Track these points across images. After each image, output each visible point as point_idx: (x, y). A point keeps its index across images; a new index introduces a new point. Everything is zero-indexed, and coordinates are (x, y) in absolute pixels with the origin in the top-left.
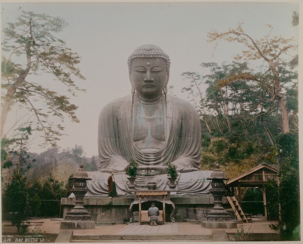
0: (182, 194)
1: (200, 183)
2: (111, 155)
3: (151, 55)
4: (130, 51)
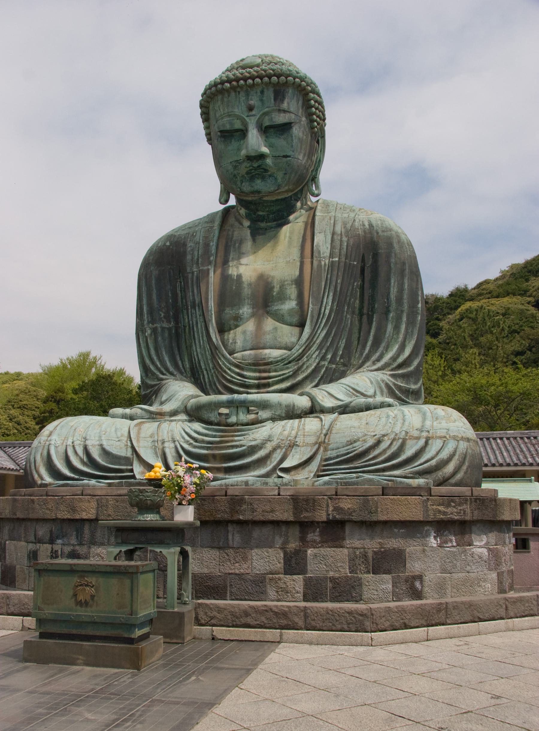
0: (327, 478)
1: (394, 443)
2: (161, 376)
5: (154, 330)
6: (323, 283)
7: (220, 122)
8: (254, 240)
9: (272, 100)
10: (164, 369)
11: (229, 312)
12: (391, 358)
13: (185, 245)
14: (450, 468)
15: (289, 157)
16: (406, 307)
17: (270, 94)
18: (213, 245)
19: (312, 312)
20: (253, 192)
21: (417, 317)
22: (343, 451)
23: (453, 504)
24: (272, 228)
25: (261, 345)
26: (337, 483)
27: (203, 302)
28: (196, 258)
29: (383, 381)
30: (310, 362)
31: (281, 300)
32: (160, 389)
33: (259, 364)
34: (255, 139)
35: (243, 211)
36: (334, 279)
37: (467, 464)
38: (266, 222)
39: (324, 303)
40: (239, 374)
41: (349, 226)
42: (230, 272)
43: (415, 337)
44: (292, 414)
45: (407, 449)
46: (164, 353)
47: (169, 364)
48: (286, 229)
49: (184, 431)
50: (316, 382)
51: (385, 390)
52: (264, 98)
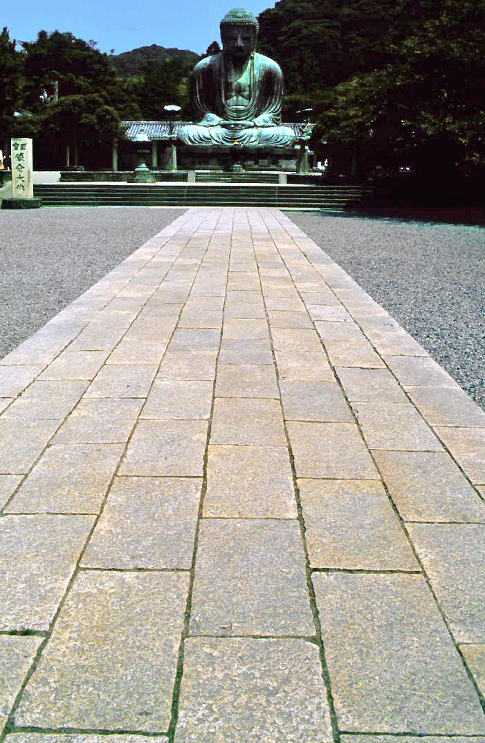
14: (288, 143)
17: (245, 29)
33: (238, 111)
44: (250, 127)
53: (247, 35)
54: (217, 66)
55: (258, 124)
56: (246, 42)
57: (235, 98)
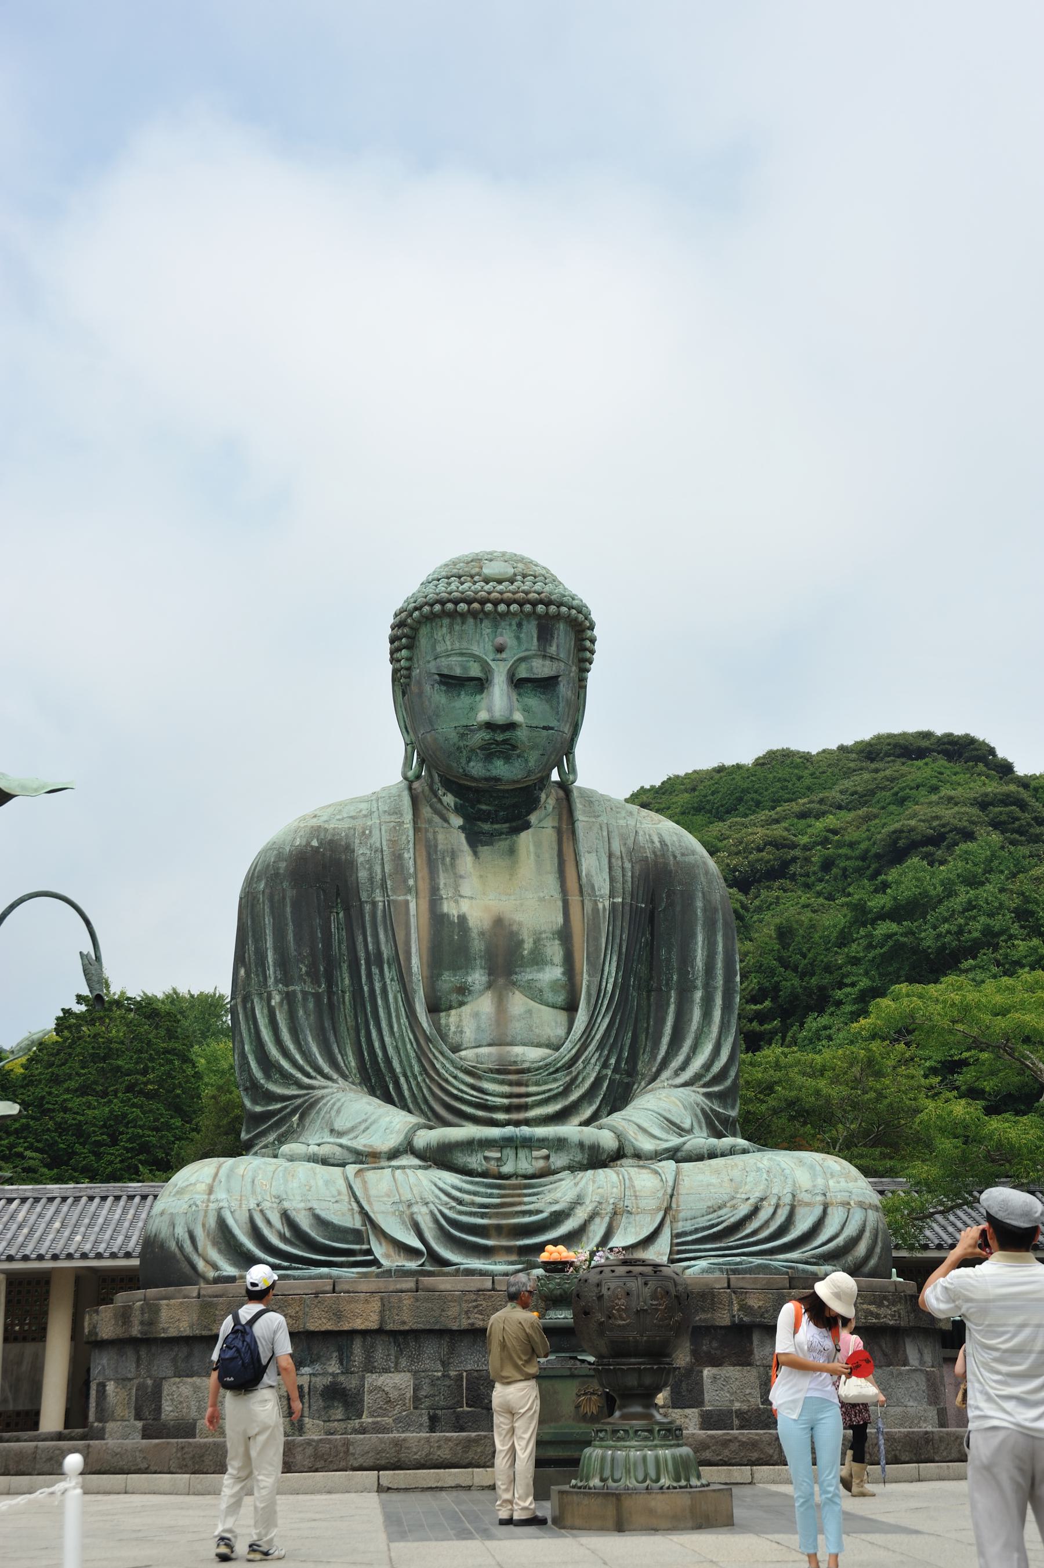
0: (703, 1264)
1: (780, 1211)
2: (306, 1080)
3: (515, 601)
4: (404, 585)
5: (289, 998)
6: (604, 940)
7: (444, 662)
8: (475, 854)
9: (535, 640)
10: (311, 1067)
11: (448, 980)
12: (703, 1067)
13: (349, 849)
15: (552, 728)
16: (719, 981)
17: (531, 629)
18: (408, 855)
19: (588, 987)
20: (487, 779)
21: (734, 998)
22: (703, 1222)
23: (886, 1303)
24: (501, 834)
25: (509, 1039)
26: (721, 1270)
27: (401, 957)
28: (379, 877)
29: (698, 1105)
30: (587, 1071)
31: (537, 964)
32: (312, 1105)
34: (505, 698)
35: (449, 799)
36: (618, 932)
37: (880, 1244)
38: (492, 823)
39: (606, 973)
40: (473, 1087)
41: (630, 842)
42: (445, 910)
43: (733, 1030)
44: (597, 1159)
45: (797, 1221)
46: (310, 1039)
47: (321, 1061)
48: (525, 838)
49: (436, 1185)
50: (598, 1103)
51: (703, 1120)
52: (522, 635)
53: (542, 668)
54: (380, 838)
55: (647, 1145)
56: (533, 702)
57: (484, 1005)
